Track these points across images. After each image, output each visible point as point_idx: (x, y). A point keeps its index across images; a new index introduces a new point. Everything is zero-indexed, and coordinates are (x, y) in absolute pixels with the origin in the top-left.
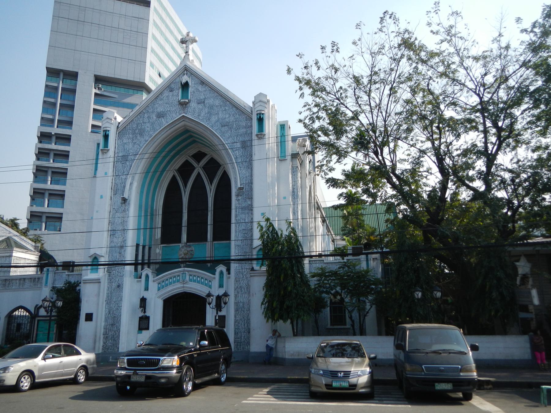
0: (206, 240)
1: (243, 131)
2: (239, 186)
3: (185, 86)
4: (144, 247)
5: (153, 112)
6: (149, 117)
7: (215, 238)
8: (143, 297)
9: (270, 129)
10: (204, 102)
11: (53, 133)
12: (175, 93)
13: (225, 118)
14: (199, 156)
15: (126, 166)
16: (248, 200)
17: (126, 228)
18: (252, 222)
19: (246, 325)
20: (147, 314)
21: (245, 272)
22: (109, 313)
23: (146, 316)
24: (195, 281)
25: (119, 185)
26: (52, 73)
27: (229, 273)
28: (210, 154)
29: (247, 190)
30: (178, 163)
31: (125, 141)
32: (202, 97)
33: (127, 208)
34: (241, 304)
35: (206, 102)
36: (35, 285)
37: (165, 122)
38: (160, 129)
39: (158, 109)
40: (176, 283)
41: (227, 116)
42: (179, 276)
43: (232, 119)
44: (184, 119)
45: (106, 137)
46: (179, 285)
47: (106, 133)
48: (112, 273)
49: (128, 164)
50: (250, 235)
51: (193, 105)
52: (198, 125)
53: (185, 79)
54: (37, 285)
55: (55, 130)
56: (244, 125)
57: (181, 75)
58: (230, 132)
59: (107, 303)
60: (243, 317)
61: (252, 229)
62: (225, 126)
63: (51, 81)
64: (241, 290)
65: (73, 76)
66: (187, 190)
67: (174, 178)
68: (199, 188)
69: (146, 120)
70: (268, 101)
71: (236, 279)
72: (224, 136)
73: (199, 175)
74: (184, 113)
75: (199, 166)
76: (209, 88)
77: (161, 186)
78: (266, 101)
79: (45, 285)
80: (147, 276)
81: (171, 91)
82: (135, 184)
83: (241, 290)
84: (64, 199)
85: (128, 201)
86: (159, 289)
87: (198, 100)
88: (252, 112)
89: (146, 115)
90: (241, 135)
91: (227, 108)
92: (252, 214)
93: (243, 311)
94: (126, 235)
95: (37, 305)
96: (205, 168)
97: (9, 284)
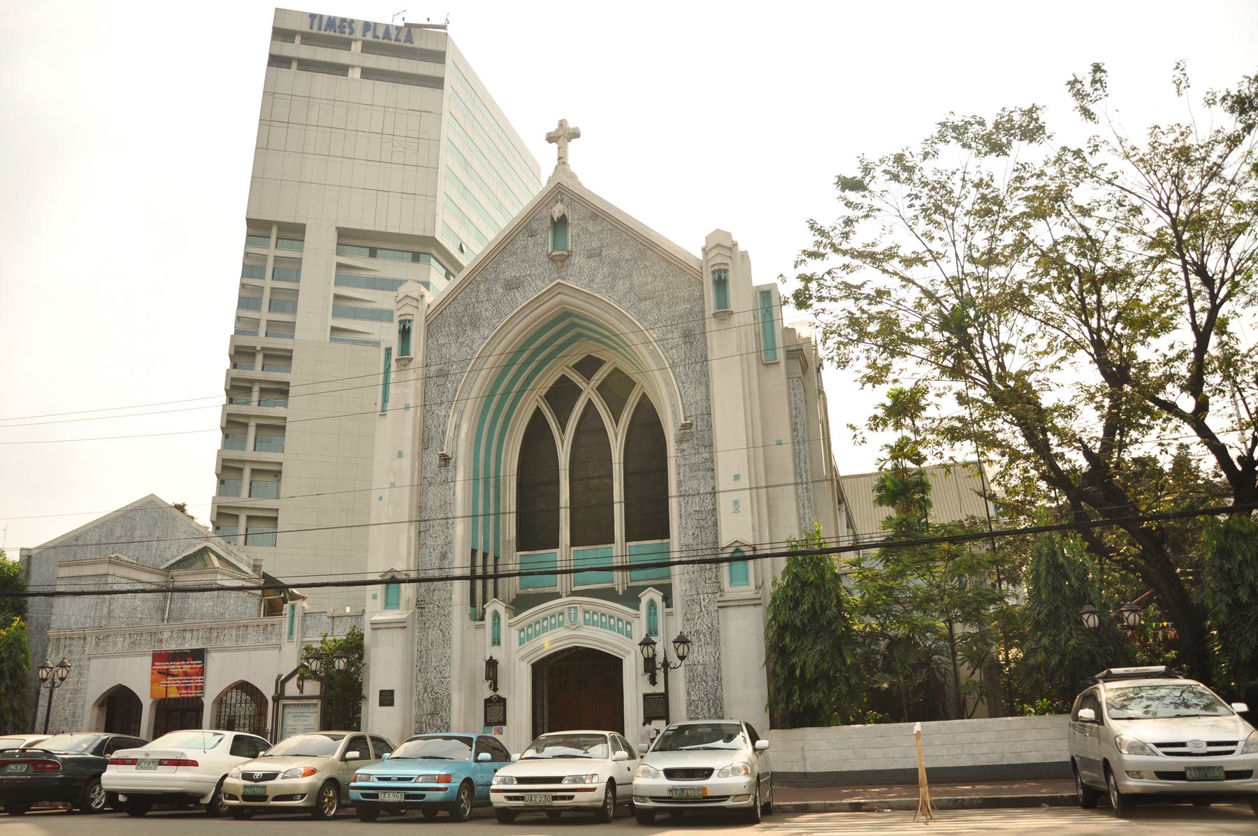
1: (683, 307)
2: (683, 422)
3: (560, 224)
4: (485, 555)
5: (496, 280)
6: (488, 291)
8: (491, 657)
9: (740, 301)
10: (600, 254)
11: (259, 348)
12: (538, 238)
13: (647, 284)
14: (588, 366)
15: (446, 390)
16: (702, 450)
17: (450, 515)
18: (715, 493)
19: (712, 710)
20: (501, 693)
21: (704, 600)
22: (425, 691)
23: (499, 697)
24: (594, 624)
25: (433, 430)
26: (257, 228)
27: (669, 605)
28: (612, 361)
29: (699, 428)
30: (548, 380)
31: (442, 341)
33: (451, 474)
34: (700, 668)
35: (604, 254)
37: (522, 299)
38: (511, 312)
39: (507, 273)
40: (558, 629)
41: (650, 279)
42: (561, 613)
43: (660, 284)
44: (560, 290)
45: (405, 333)
46: (562, 632)
47: (404, 326)
48: (427, 610)
49: (449, 385)
50: (710, 523)
51: (578, 260)
52: (591, 301)
53: (558, 210)
55: (260, 341)
56: (686, 295)
57: (552, 203)
59: (420, 671)
60: (707, 695)
61: (714, 509)
62: (646, 299)
63: (255, 245)
64: (698, 637)
65: (294, 232)
66: (567, 437)
67: (538, 412)
68: (591, 430)
69: (483, 296)
70: (735, 245)
71: (686, 614)
72: (645, 320)
73: (590, 402)
74: (560, 277)
75: (590, 386)
76: (610, 226)
77: (512, 431)
78: (729, 244)
79: (289, 638)
80: (496, 615)
81: (531, 236)
82: (465, 427)
83: (698, 637)
84: (279, 481)
85: (452, 461)
87: (587, 251)
88: (701, 267)
89: (482, 286)
90: (681, 317)
91: (647, 263)
92: (713, 478)
93: (705, 681)
94: (451, 531)
95: (280, 676)
96: (601, 389)
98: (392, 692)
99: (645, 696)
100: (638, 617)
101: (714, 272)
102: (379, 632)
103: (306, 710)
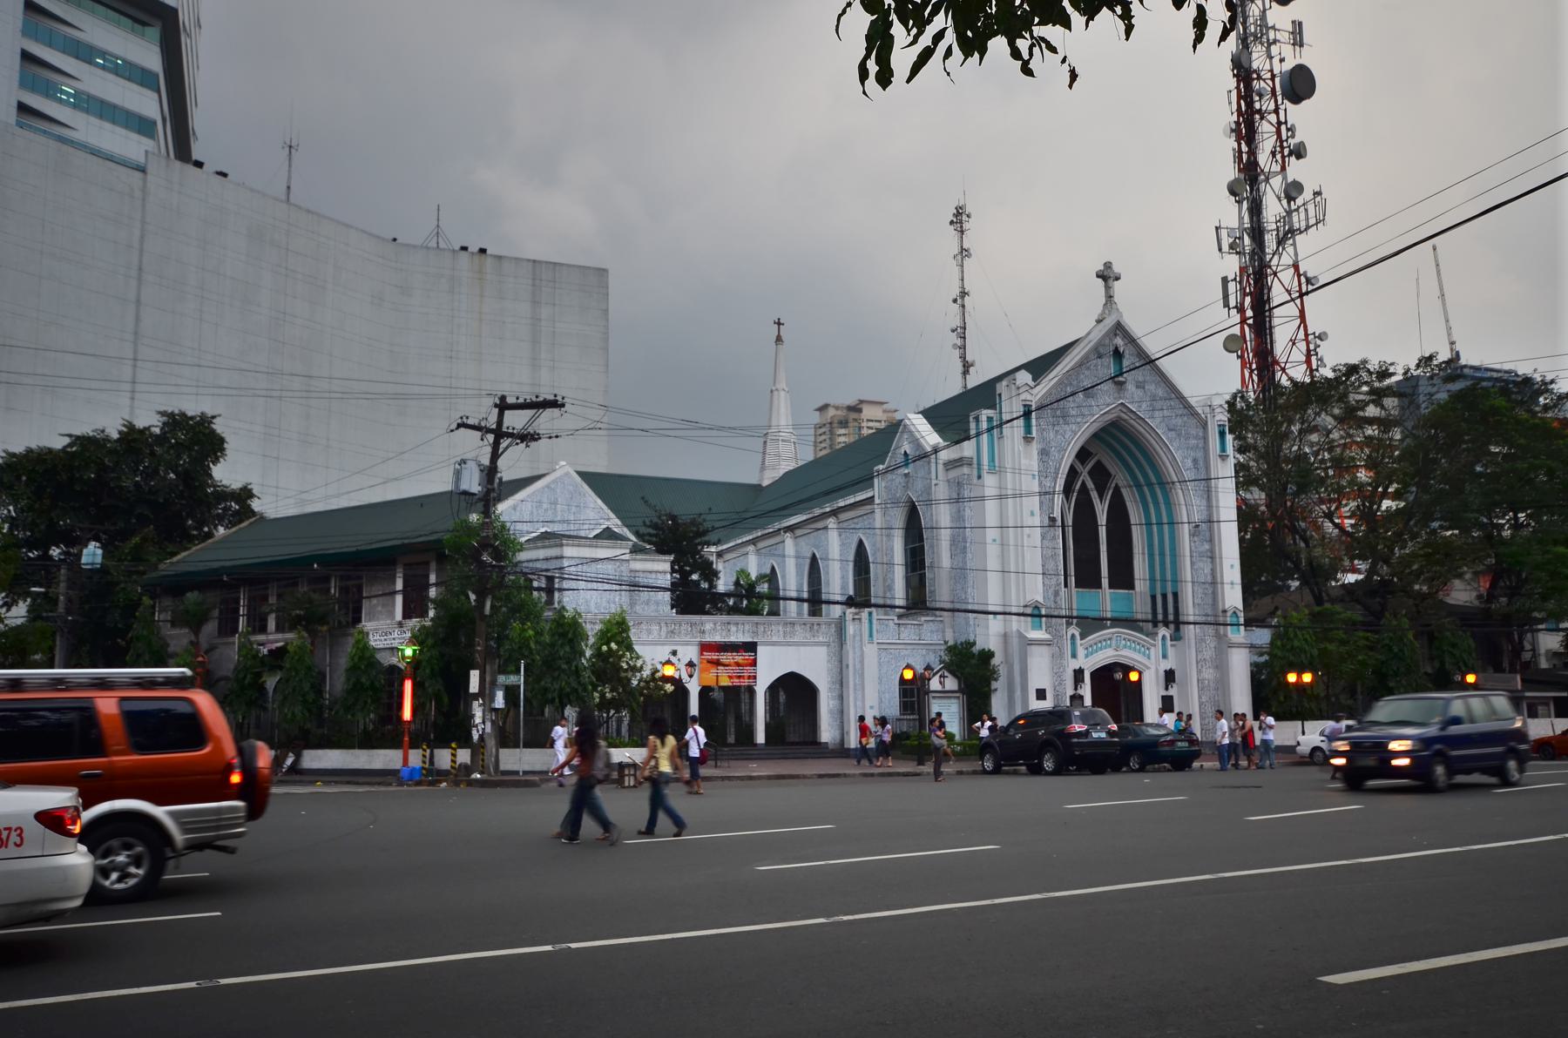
0: (1099, 586)
7: (1111, 586)
10: (1144, 388)
24: (1130, 648)
32: (1141, 379)
34: (1207, 682)
35: (1146, 387)
36: (814, 636)
42: (1110, 639)
52: (1140, 422)
54: (818, 637)
58: (1178, 440)
74: (1120, 398)
86: (1087, 656)
97: (764, 631)
98: (1044, 690)
99: (1163, 697)
100: (1155, 646)
101: (1220, 426)
102: (1033, 647)
103: (949, 701)
